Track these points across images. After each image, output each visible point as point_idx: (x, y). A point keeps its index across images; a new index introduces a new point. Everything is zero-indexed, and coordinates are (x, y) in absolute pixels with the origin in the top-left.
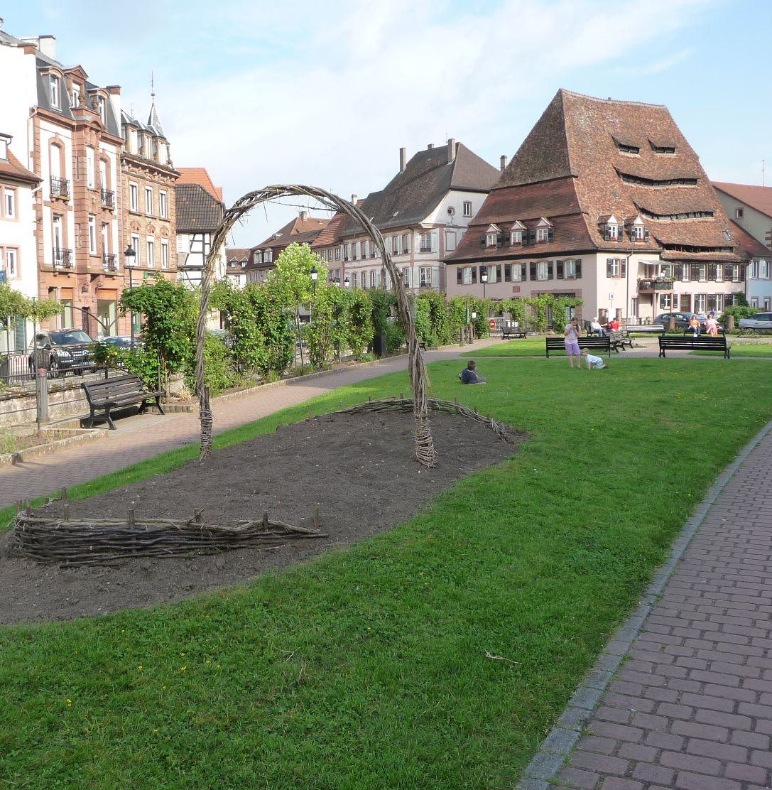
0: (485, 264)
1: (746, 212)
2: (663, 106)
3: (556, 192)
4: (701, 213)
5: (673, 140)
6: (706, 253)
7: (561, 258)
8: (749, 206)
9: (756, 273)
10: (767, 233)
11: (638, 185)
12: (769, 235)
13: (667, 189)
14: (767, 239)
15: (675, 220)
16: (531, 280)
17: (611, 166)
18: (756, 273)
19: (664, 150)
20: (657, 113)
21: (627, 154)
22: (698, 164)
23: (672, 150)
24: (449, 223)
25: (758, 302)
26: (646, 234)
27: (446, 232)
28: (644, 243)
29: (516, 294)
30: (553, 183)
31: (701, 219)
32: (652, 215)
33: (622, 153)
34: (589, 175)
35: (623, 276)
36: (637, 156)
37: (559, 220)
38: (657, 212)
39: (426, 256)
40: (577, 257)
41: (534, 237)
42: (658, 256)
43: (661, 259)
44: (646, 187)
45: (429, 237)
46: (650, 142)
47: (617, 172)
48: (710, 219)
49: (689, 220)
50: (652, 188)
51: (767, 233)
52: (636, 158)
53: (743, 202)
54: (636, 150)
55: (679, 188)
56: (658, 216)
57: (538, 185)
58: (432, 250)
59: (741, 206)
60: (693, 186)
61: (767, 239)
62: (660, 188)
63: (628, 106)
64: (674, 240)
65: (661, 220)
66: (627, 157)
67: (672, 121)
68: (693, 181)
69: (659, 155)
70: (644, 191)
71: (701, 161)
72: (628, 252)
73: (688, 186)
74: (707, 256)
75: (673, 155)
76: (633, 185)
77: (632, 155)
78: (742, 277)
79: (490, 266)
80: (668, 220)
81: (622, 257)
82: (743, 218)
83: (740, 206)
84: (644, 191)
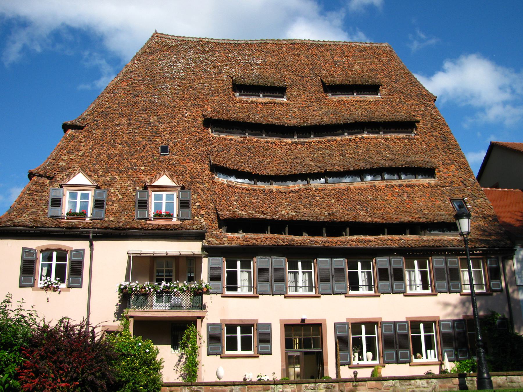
13: (329, 141)
21: (254, 99)
36: (278, 100)
44: (274, 139)
50: (289, 141)
52: (274, 103)
65: (275, 187)
66: (252, 102)
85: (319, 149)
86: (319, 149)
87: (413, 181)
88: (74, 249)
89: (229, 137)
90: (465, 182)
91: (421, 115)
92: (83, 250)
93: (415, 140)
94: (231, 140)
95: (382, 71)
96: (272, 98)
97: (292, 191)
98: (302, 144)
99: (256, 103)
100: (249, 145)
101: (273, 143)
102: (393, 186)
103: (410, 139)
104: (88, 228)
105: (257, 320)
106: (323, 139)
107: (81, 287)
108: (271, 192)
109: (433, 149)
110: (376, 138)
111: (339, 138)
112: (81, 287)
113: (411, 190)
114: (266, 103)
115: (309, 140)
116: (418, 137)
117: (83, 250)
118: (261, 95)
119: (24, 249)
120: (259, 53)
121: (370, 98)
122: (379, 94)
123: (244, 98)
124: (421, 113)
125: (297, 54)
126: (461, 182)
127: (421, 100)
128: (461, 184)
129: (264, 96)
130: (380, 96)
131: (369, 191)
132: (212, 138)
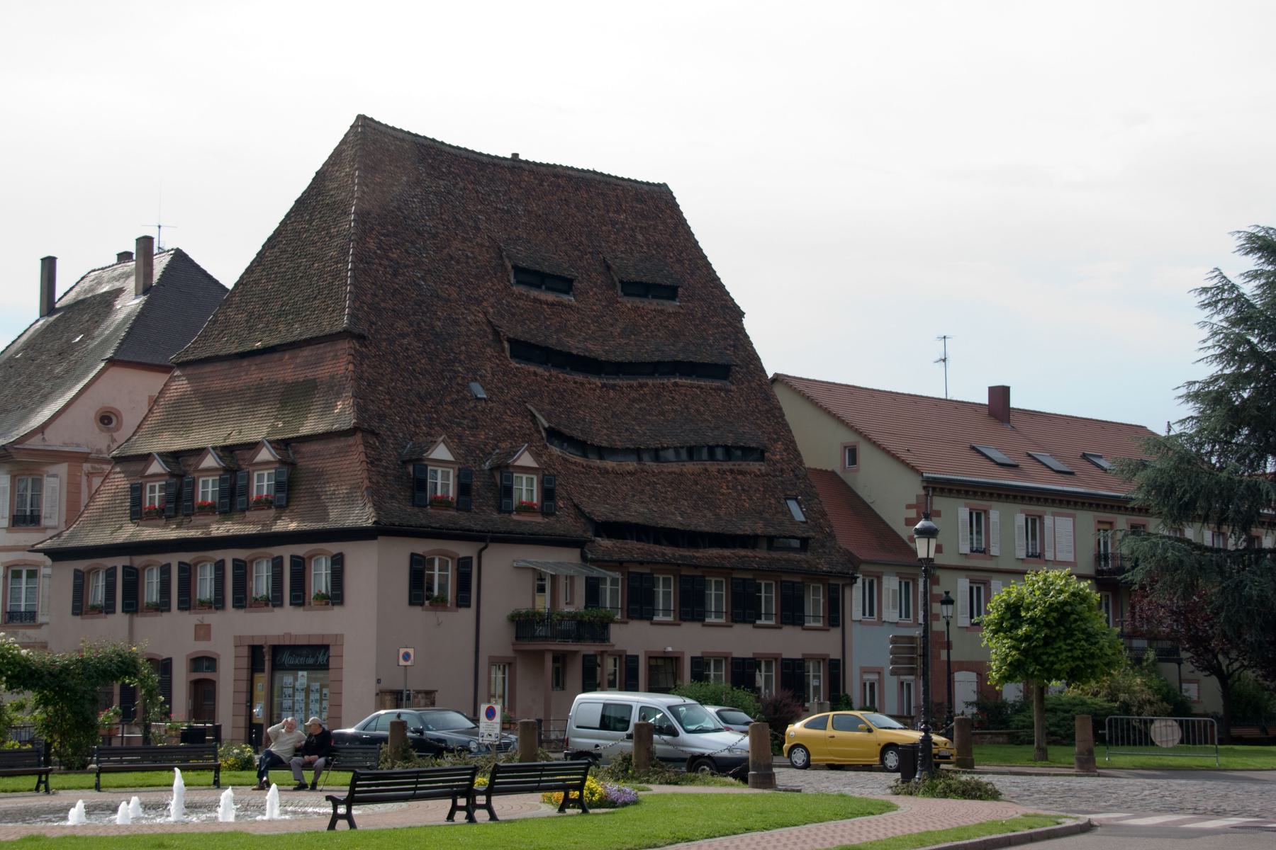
0: (139, 561)
1: (864, 451)
2: (665, 185)
3: (310, 374)
4: (729, 452)
5: (677, 267)
6: (727, 552)
7: (301, 550)
9: (871, 606)
10: (909, 507)
11: (554, 372)
13: (641, 386)
15: (650, 465)
16: (234, 606)
18: (871, 606)
21: (534, 293)
22: (742, 330)
23: (670, 292)
24: (99, 451)
25: (881, 681)
26: (548, 494)
27: (90, 475)
28: (539, 519)
29: (202, 647)
30: (306, 352)
31: (727, 466)
32: (583, 447)
33: (521, 289)
34: (403, 336)
35: (463, 600)
36: (565, 298)
37: (306, 448)
39: (26, 537)
40: (334, 548)
41: (246, 490)
42: (577, 552)
43: (584, 558)
44: (580, 378)
45: (38, 484)
46: (609, 268)
47: (496, 333)
48: (755, 466)
49: (690, 467)
50: (598, 381)
51: (909, 507)
52: (560, 304)
54: (564, 284)
55: (676, 384)
56: (601, 452)
57: (276, 356)
58: (44, 522)
59: (850, 438)
60: (717, 384)
62: (621, 382)
64: (636, 512)
65: (609, 464)
66: (536, 300)
68: (720, 371)
69: (629, 302)
70: (572, 385)
71: (749, 324)
72: (486, 538)
74: (724, 558)
75: (671, 306)
76: (540, 370)
77: (550, 297)
78: (835, 616)
79: (148, 566)
80: (631, 465)
81: (464, 550)
82: (857, 470)
83: (850, 438)
84: (572, 385)
85: (634, 400)
86: (634, 400)
87: (744, 466)
88: (461, 556)
89: (532, 368)
90: (797, 472)
92: (471, 558)
94: (535, 374)
95: (671, 249)
96: (557, 294)
99: (541, 302)
101: (582, 384)
103: (728, 391)
105: (625, 651)
106: (635, 383)
107: (469, 606)
108: (607, 472)
109: (754, 411)
110: (692, 386)
111: (650, 382)
112: (469, 606)
114: (553, 304)
115: (619, 382)
117: (471, 558)
118: (544, 287)
119: (412, 555)
125: (565, 200)
127: (728, 318)
129: (549, 289)
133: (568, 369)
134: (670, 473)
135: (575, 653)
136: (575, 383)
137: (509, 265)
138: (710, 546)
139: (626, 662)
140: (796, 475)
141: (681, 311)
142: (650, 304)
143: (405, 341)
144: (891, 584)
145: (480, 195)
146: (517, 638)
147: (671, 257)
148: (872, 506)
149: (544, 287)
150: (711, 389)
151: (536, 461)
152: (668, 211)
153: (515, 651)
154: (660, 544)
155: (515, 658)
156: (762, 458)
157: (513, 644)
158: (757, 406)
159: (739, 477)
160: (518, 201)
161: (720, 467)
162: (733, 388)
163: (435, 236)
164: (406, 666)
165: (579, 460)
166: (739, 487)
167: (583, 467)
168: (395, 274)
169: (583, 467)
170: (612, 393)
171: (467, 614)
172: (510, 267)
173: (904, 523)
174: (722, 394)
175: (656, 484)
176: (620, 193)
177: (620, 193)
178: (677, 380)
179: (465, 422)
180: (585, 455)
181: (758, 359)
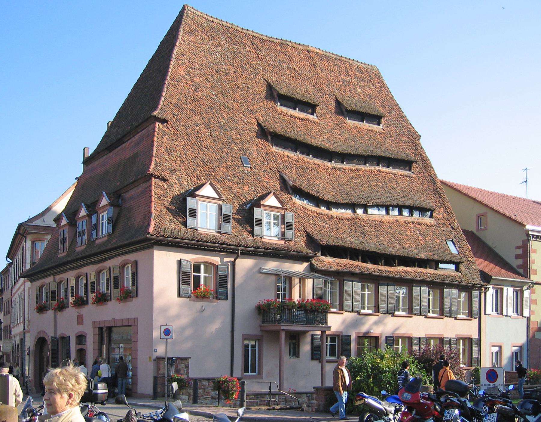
8: (493, 210)
10: (517, 248)
11: (301, 156)
12: (520, 251)
13: (357, 170)
14: (517, 257)
17: (254, 121)
19: (361, 116)
20: (362, 73)
21: (291, 112)
32: (317, 201)
36: (311, 117)
38: (328, 197)
44: (318, 161)
51: (517, 248)
52: (307, 120)
53: (486, 206)
55: (379, 171)
56: (329, 205)
59: (482, 210)
60: (405, 172)
61: (517, 257)
63: (308, 52)
65: (334, 212)
67: (383, 85)
68: (407, 164)
69: (351, 123)
71: (423, 142)
73: (396, 171)
77: (302, 115)
84: (312, 165)
85: (352, 178)
91: (413, 153)
93: (414, 179)
97: (347, 219)
98: (339, 169)
100: (303, 165)
101: (319, 165)
102: (409, 222)
103: (411, 177)
104: (240, 246)
108: (332, 217)
109: (426, 190)
113: (420, 227)
116: (415, 175)
118: (297, 109)
120: (283, 56)
121: (375, 127)
122: (381, 125)
123: (284, 109)
124: (413, 151)
126: (450, 224)
128: (449, 226)
130: (382, 128)
131: (395, 225)
132: (274, 153)
133: (311, 156)
134: (375, 221)
135: (305, 332)
136: (315, 164)
137: (275, 94)
138: (399, 265)
139: (342, 339)
140: (452, 227)
141: (384, 132)
142: (365, 125)
143: (198, 128)
144: (509, 292)
145: (260, 56)
146: (263, 322)
147: (378, 103)
148: (495, 249)
149: (297, 109)
150: (401, 175)
151: (280, 202)
152: (376, 79)
153: (262, 331)
154: (366, 262)
155: (262, 336)
156: (431, 217)
157: (261, 326)
158: (428, 186)
159: (418, 226)
160: (284, 62)
161: (406, 220)
162: (414, 176)
163: (227, 74)
164: (167, 339)
165: (314, 209)
166: (418, 232)
167: (317, 214)
168: (196, 90)
169: (317, 214)
170: (338, 172)
171: (226, 305)
172: (276, 96)
173: (514, 257)
174: (408, 179)
175: (365, 226)
176: (348, 66)
177: (348, 66)
178: (380, 169)
179: (235, 179)
180: (318, 206)
181: (429, 160)
